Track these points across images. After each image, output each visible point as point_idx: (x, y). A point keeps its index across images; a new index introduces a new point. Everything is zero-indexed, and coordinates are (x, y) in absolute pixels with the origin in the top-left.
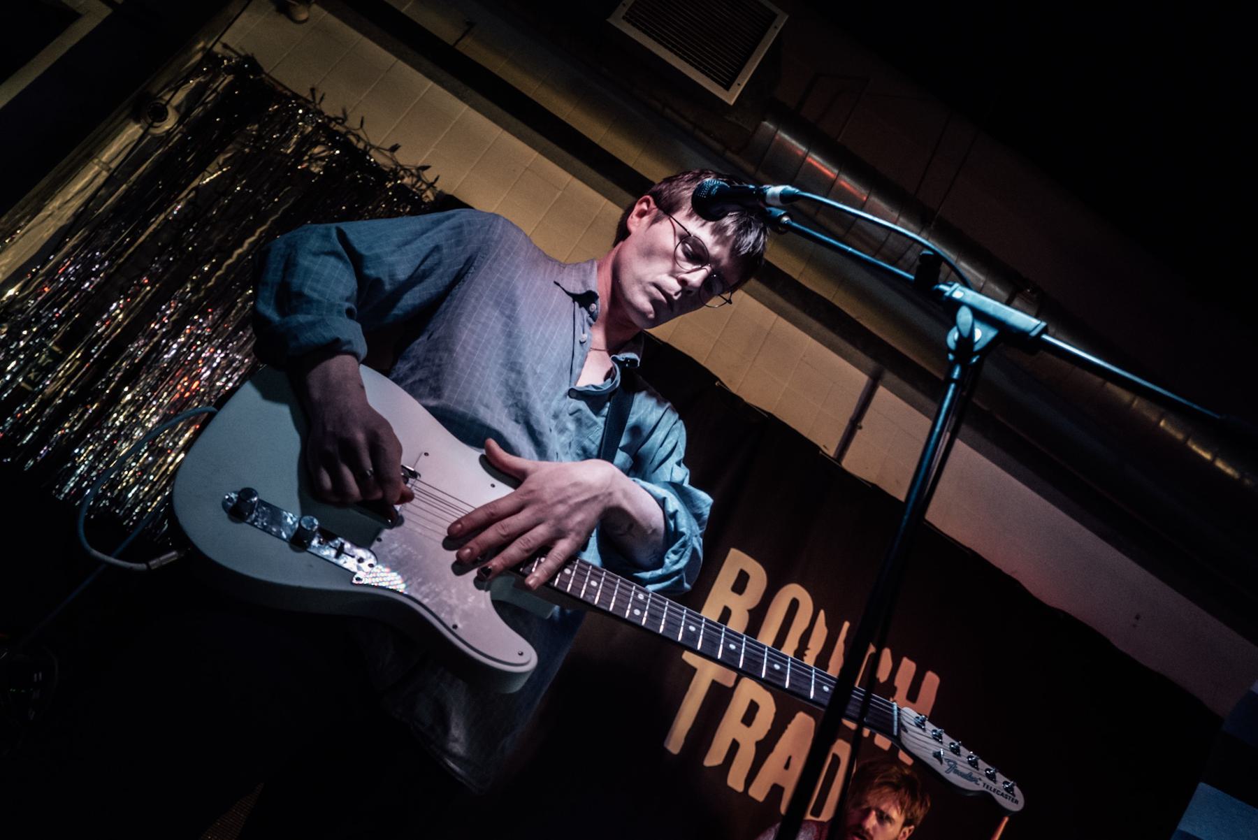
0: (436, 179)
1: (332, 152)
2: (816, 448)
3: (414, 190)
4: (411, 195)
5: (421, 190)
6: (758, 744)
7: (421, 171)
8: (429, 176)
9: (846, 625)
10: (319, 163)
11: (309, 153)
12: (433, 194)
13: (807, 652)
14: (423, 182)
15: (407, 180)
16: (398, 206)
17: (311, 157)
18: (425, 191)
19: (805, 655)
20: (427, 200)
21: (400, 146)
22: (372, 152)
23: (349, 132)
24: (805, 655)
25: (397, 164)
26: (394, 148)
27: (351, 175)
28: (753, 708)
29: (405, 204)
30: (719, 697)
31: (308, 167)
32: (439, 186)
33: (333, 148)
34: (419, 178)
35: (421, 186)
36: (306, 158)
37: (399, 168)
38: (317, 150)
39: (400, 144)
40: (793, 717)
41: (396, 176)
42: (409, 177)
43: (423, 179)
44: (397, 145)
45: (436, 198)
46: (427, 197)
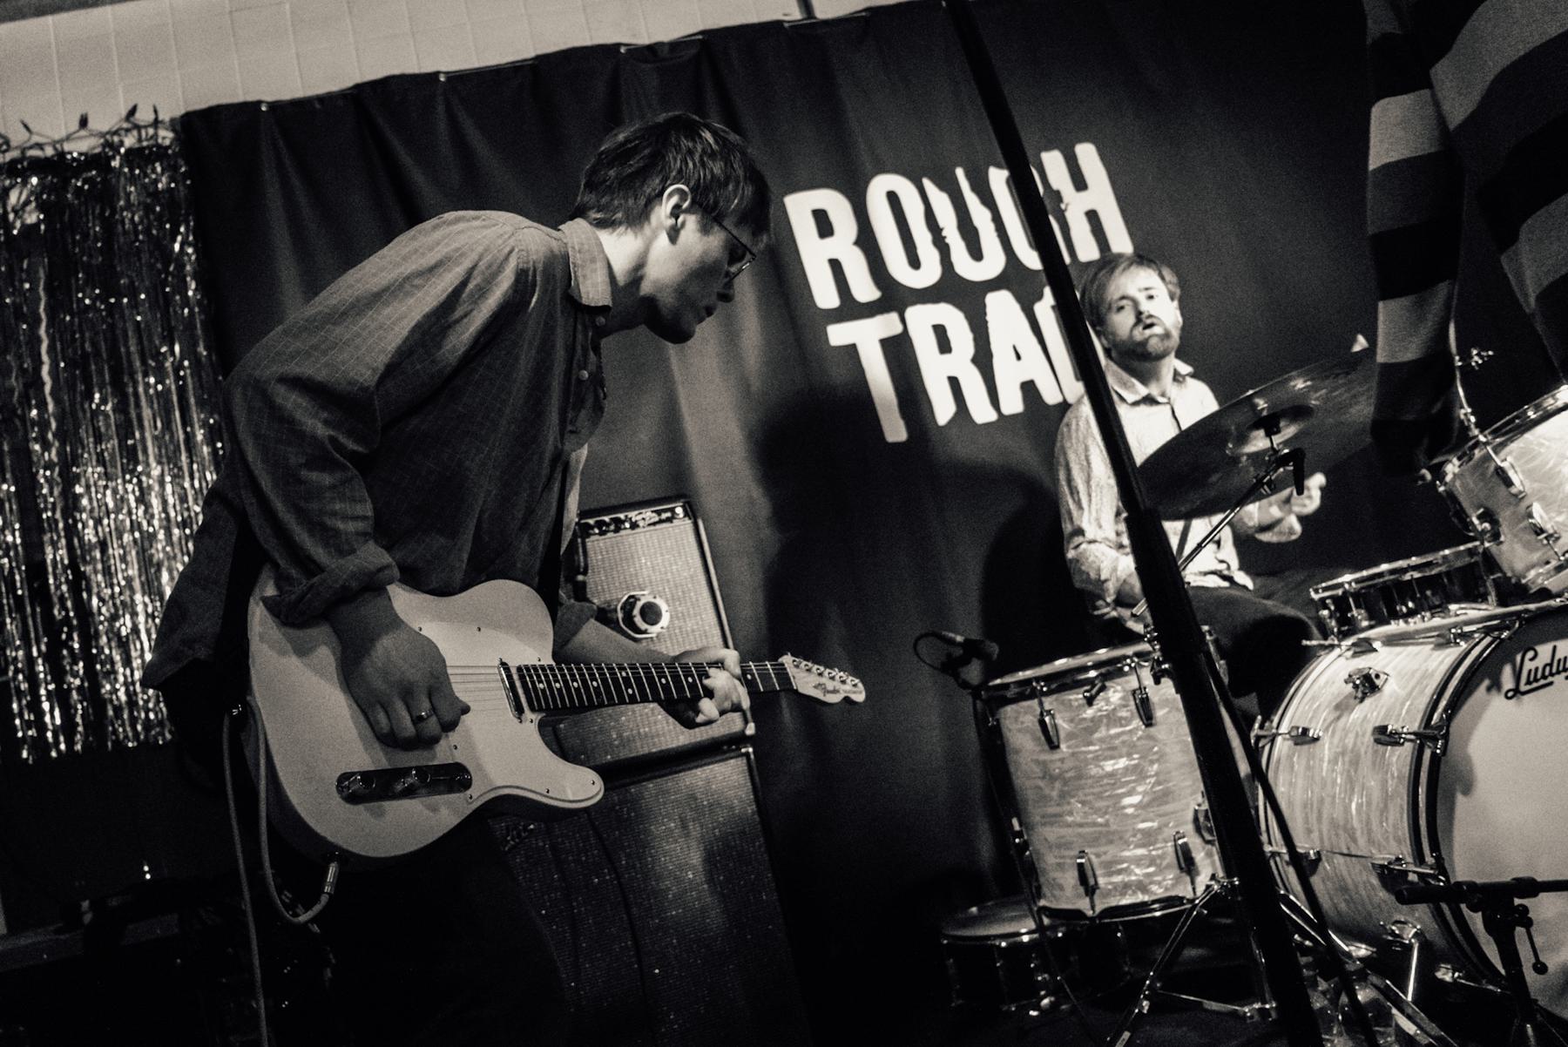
0: (156, 112)
1: (29, 186)
2: (777, 25)
3: (145, 144)
4: (147, 152)
5: (152, 137)
6: (975, 360)
7: (132, 119)
8: (145, 116)
9: (960, 172)
10: (28, 208)
11: (9, 209)
12: (167, 129)
13: (944, 234)
14: (146, 127)
15: (130, 141)
16: (146, 175)
17: (15, 211)
18: (155, 136)
19: (945, 237)
20: (167, 142)
21: (86, 115)
22: (67, 147)
23: (23, 151)
24: (945, 237)
25: (103, 135)
26: (84, 122)
27: (70, 189)
28: (940, 332)
29: (150, 167)
30: (898, 351)
31: (23, 225)
32: (165, 116)
33: (25, 183)
34: (138, 127)
35: (147, 134)
36: (11, 216)
37: (108, 137)
38: (13, 198)
39: (84, 112)
40: (984, 306)
41: (115, 148)
42: (126, 136)
43: (142, 124)
44: (82, 116)
45: (174, 130)
46: (164, 138)
